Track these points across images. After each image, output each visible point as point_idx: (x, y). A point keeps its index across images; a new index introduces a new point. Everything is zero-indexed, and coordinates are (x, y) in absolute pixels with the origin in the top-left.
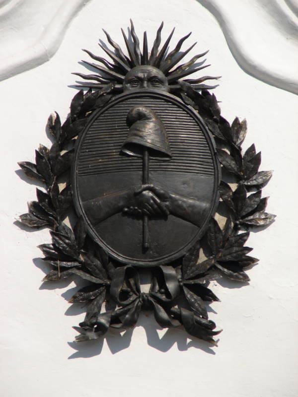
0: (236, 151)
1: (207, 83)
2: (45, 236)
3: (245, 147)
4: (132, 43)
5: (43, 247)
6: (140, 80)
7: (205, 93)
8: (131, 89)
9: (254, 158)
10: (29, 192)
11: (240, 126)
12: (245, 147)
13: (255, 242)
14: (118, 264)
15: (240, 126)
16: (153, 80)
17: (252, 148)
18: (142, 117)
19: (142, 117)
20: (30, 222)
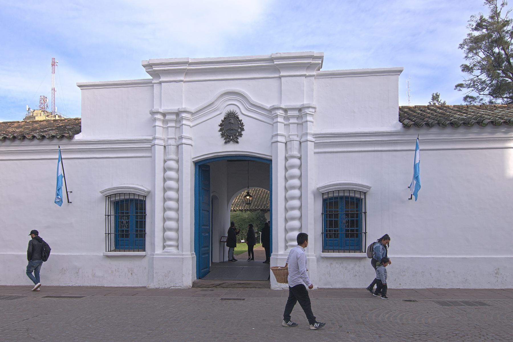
0: (241, 123)
3: (242, 122)
8: (230, 117)
10: (219, 128)
11: (241, 120)
12: (242, 122)
13: (243, 133)
14: (228, 135)
19: (231, 119)
20: (219, 131)
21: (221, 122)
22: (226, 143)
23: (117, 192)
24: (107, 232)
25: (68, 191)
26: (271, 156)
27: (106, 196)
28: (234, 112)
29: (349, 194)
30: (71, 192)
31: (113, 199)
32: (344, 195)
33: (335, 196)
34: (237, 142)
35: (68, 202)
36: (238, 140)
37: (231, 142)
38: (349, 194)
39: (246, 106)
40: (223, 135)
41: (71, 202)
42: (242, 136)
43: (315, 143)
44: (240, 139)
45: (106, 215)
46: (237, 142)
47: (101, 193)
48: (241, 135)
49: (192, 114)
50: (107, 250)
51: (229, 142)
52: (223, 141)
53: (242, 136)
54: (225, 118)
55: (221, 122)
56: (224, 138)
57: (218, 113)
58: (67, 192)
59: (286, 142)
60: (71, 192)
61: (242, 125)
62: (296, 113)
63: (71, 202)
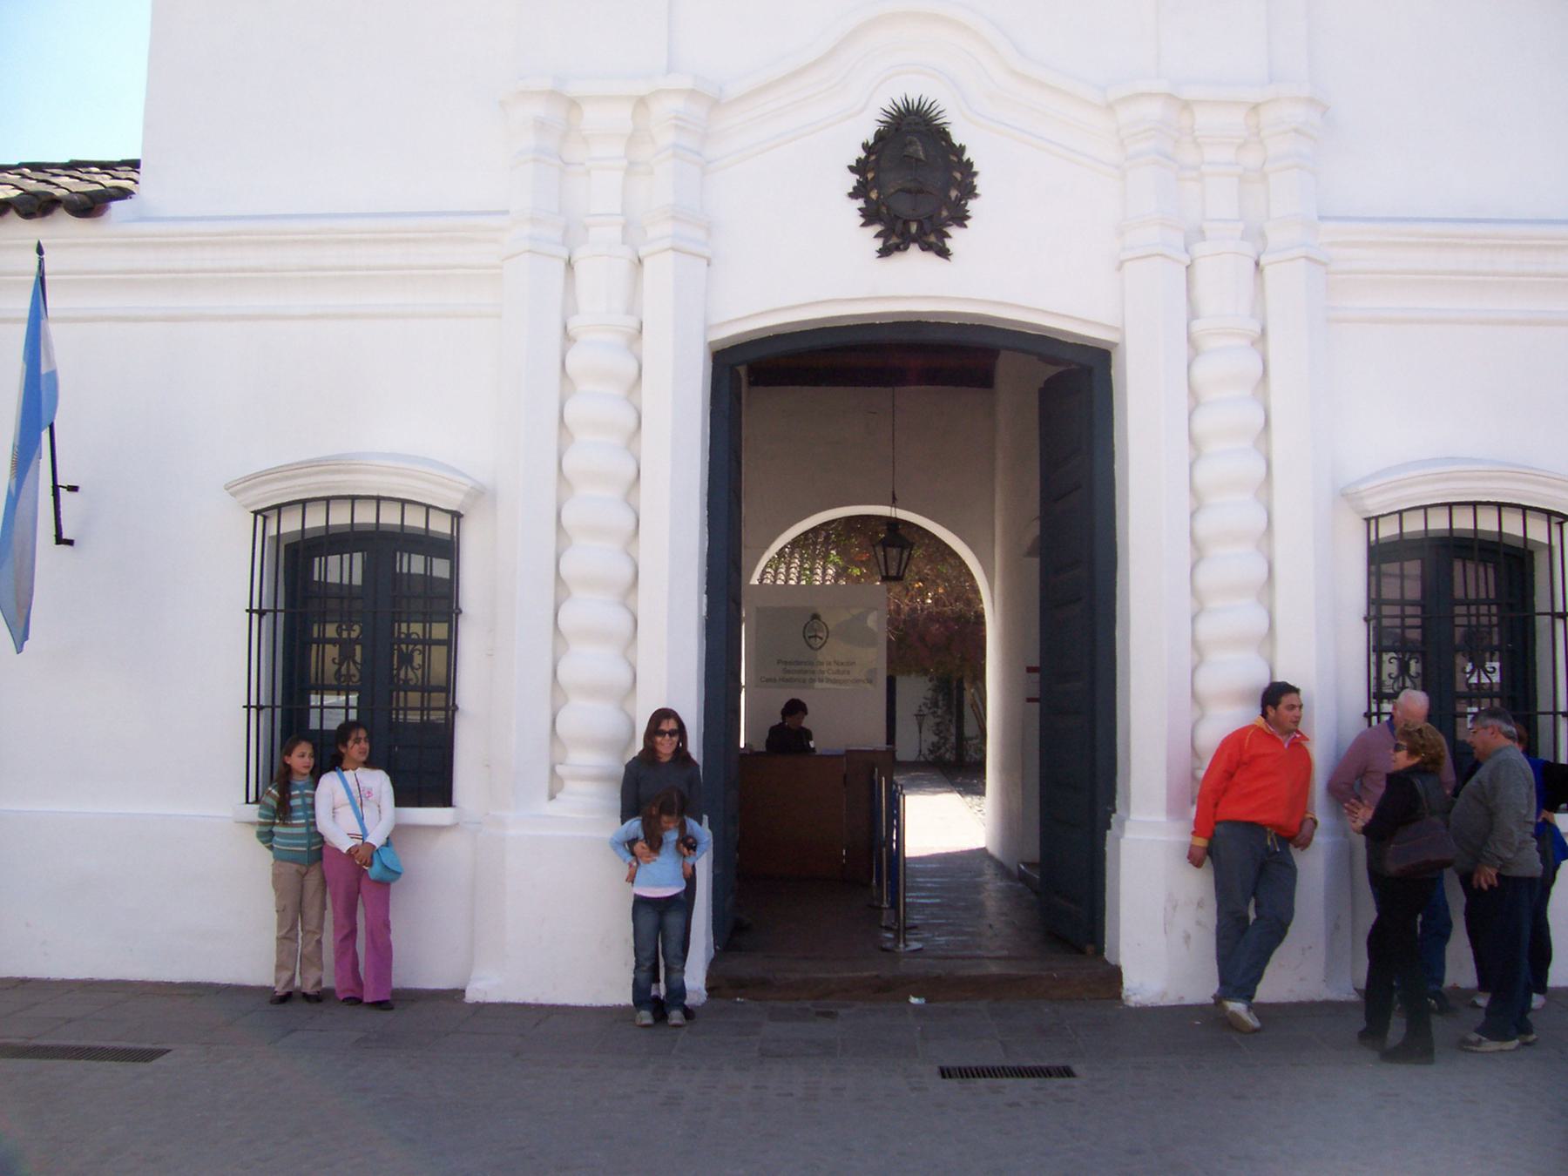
0: (960, 160)
1: (945, 126)
2: (860, 203)
4: (907, 109)
5: (860, 209)
6: (909, 124)
7: (944, 129)
9: (969, 164)
10: (852, 180)
11: (962, 149)
13: (972, 206)
15: (962, 149)
16: (917, 124)
17: (969, 159)
18: (911, 143)
21: (863, 155)
22: (885, 252)
24: (254, 702)
27: (256, 513)
30: (74, 489)
31: (291, 524)
33: (1433, 530)
34: (944, 253)
35: (60, 540)
36: (949, 243)
37: (914, 249)
40: (869, 216)
41: (70, 543)
42: (966, 222)
44: (957, 238)
45: (250, 611)
46: (944, 253)
48: (961, 219)
51: (901, 247)
52: (869, 239)
53: (966, 222)
54: (879, 136)
55: (863, 155)
56: (877, 228)
60: (74, 489)
61: (968, 169)
63: (70, 543)
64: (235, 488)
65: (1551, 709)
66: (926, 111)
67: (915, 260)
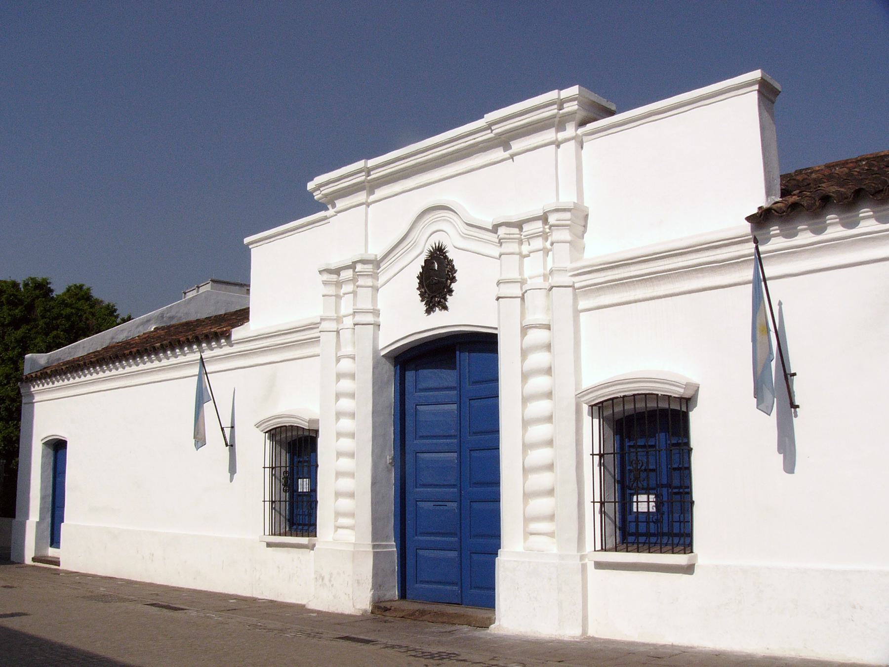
5: (419, 294)
13: (454, 286)
22: (429, 311)
23: (276, 425)
25: (223, 427)
26: (496, 329)
28: (441, 245)
29: (657, 405)
32: (658, 406)
38: (657, 405)
39: (461, 231)
43: (575, 289)
44: (451, 301)
47: (257, 427)
48: (450, 291)
49: (377, 263)
50: (267, 533)
57: (418, 252)
58: (222, 429)
59: (523, 295)
61: (453, 270)
62: (538, 226)
64: (258, 426)
65: (595, 503)
66: (438, 246)
67: (438, 313)
